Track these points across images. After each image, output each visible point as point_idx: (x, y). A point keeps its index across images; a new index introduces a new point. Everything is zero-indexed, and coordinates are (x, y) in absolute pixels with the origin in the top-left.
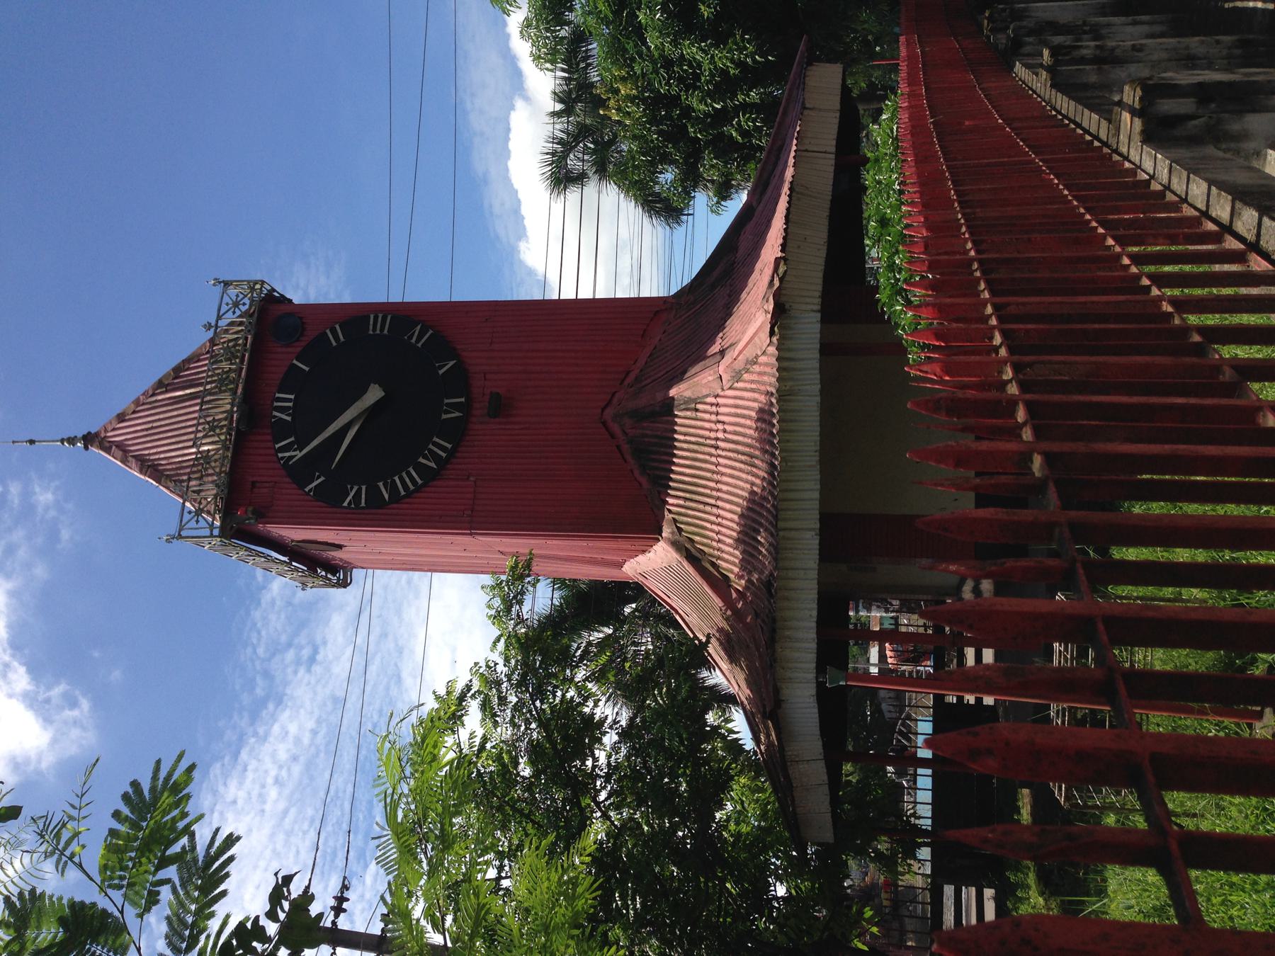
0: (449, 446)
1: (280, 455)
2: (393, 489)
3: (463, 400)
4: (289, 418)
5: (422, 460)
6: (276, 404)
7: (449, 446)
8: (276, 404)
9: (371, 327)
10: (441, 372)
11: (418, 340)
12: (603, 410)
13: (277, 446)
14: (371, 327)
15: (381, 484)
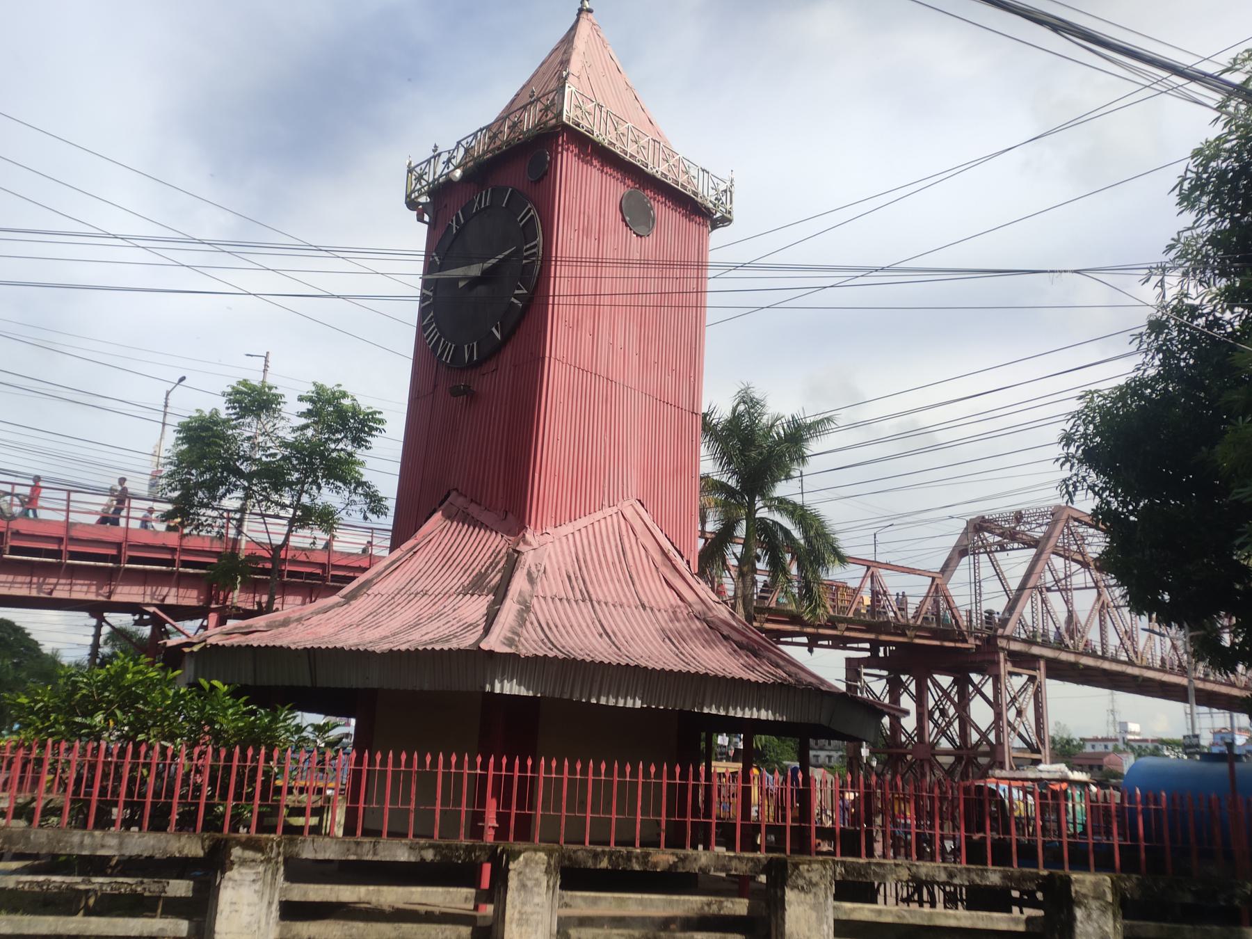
0: (448, 361)
1: (454, 218)
2: (429, 325)
3: (475, 358)
4: (474, 210)
5: (443, 339)
6: (484, 192)
7: (448, 361)
8: (484, 192)
9: (528, 246)
10: (494, 330)
11: (516, 297)
12: (456, 490)
13: (460, 212)
14: (528, 246)
15: (432, 314)
